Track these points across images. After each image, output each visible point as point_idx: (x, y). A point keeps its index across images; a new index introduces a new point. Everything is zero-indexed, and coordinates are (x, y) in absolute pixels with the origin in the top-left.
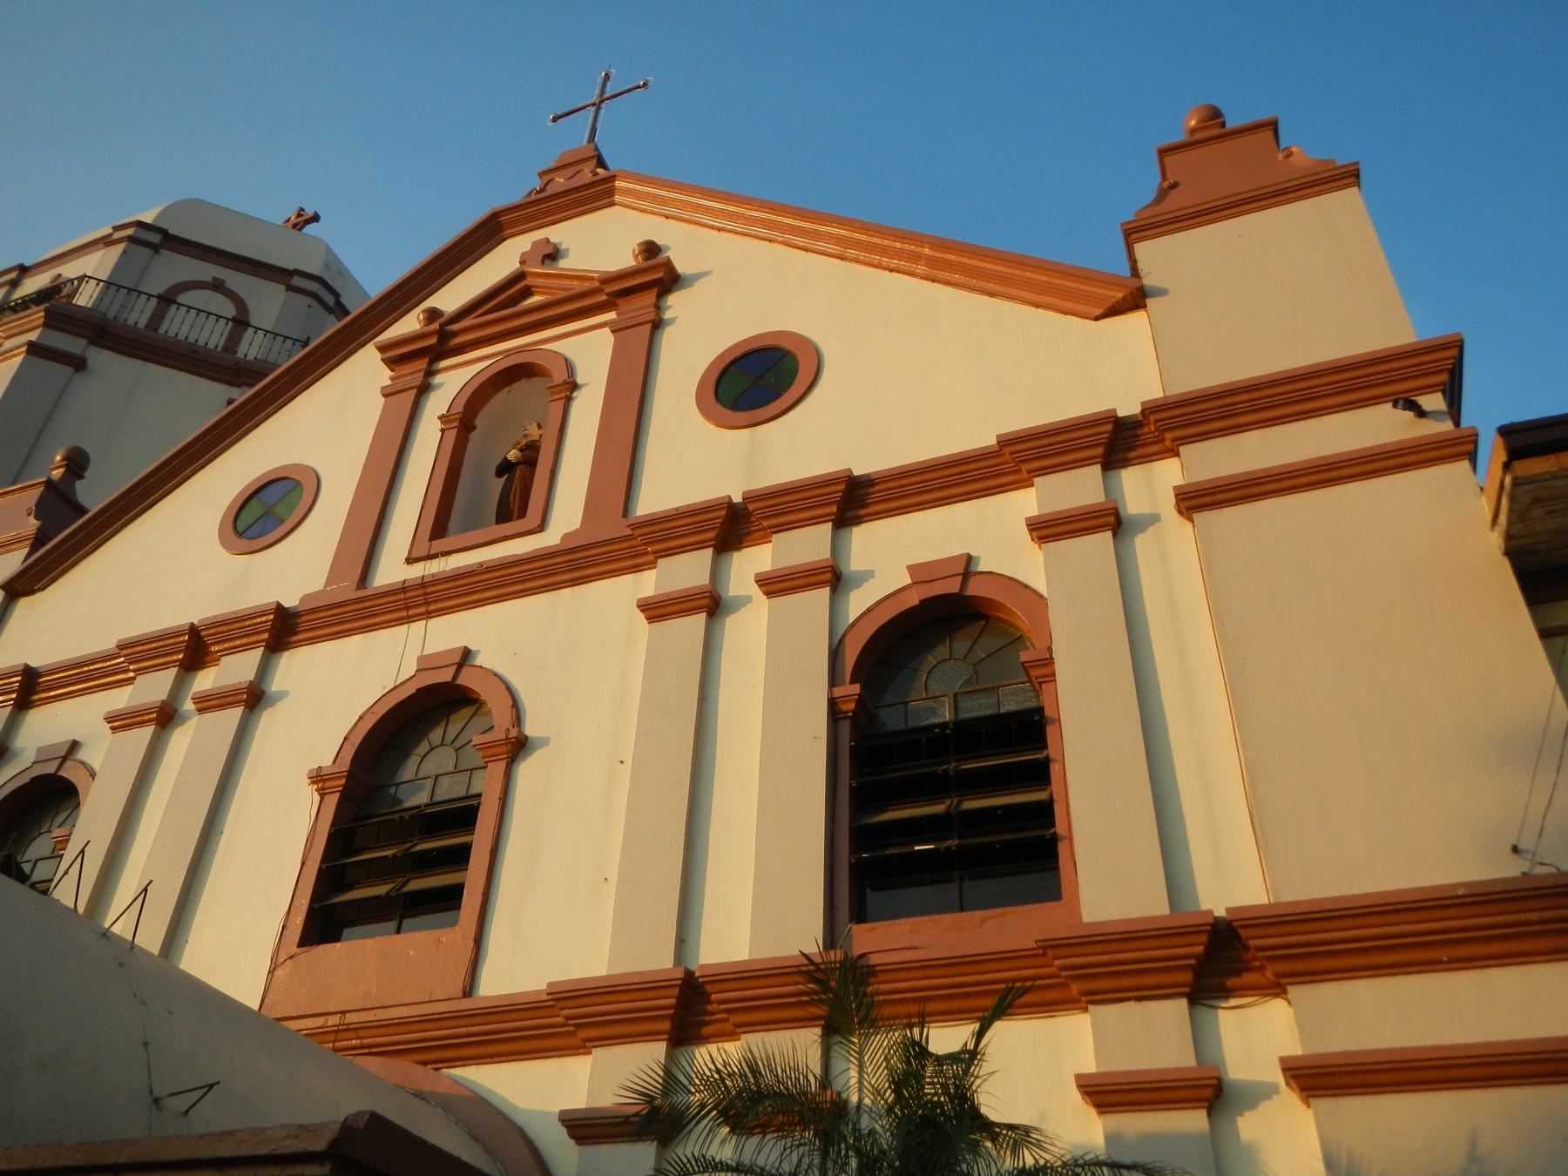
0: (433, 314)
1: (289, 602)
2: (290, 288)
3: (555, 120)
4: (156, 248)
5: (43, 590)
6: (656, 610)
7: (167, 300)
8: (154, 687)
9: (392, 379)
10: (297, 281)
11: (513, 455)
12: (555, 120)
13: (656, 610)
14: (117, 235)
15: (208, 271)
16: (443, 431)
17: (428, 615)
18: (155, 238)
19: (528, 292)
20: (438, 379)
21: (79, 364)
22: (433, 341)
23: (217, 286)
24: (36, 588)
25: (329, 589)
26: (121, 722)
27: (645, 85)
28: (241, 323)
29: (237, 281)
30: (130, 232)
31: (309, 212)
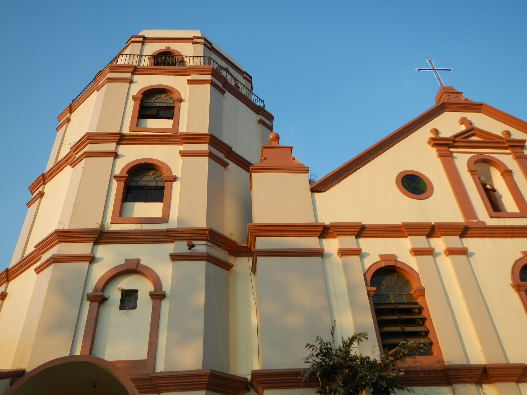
0: (436, 131)
3: (419, 70)
5: (324, 192)
8: (421, 242)
9: (438, 151)
12: (419, 70)
14: (195, 40)
16: (472, 175)
17: (512, 237)
18: (210, 46)
19: (473, 135)
22: (451, 142)
24: (322, 191)
26: (416, 252)
27: (450, 70)
30: (202, 41)
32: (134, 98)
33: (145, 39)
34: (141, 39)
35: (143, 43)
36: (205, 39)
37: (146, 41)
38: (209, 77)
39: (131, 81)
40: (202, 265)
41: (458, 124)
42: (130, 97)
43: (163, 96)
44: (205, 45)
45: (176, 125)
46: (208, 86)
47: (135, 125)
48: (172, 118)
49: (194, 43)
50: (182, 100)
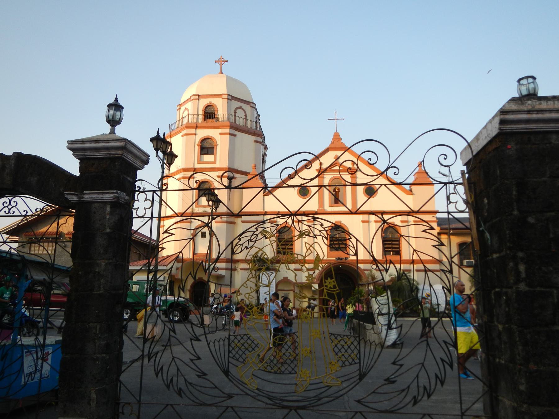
0: (321, 164)
1: (316, 210)
2: (251, 107)
4: (231, 100)
6: (363, 222)
7: (235, 112)
10: (252, 105)
11: (336, 190)
13: (363, 222)
15: (239, 104)
18: (230, 98)
19: (337, 165)
20: (325, 176)
21: (235, 135)
23: (240, 108)
25: (321, 209)
28: (246, 116)
29: (244, 106)
30: (226, 97)
31: (226, 59)
32: (198, 145)
33: (199, 96)
34: (197, 97)
35: (198, 100)
36: (228, 95)
37: (200, 97)
38: (228, 130)
39: (195, 134)
40: (225, 224)
41: (333, 158)
42: (196, 145)
43: (210, 140)
44: (228, 99)
45: (215, 159)
46: (228, 136)
47: (200, 161)
48: (213, 154)
49: (223, 99)
50: (217, 145)
